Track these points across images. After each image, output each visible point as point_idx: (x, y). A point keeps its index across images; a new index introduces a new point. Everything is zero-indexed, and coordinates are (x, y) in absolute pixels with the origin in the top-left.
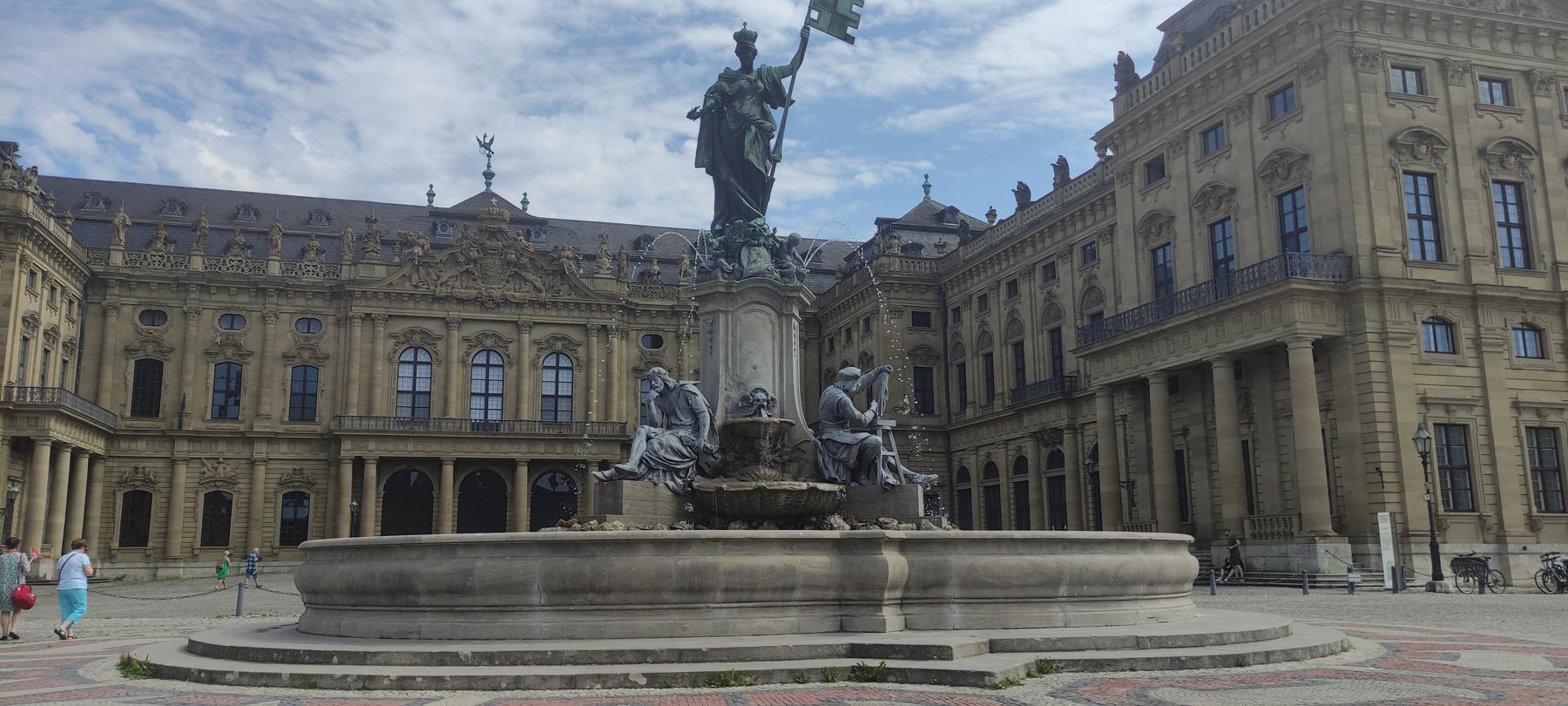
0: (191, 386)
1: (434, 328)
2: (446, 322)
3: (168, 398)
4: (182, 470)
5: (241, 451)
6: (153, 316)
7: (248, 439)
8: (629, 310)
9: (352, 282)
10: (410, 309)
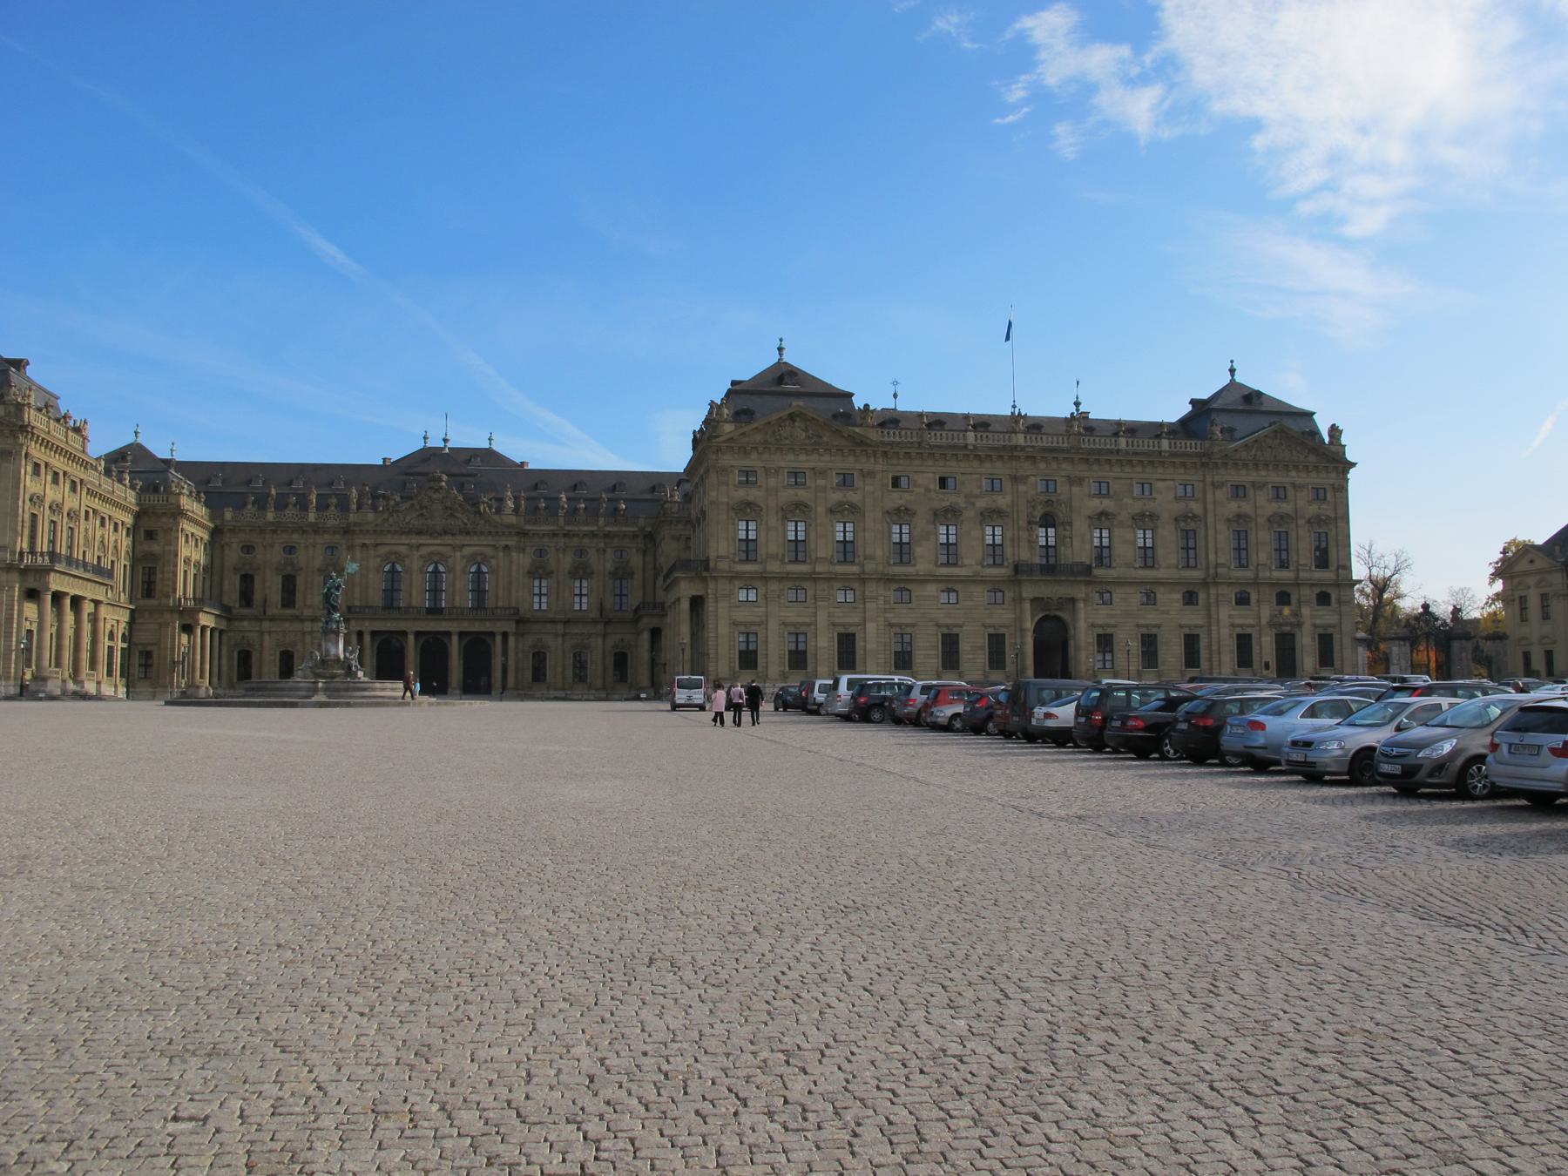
0: (269, 587)
1: (404, 550)
2: (410, 546)
3: (258, 597)
4: (266, 637)
5: (297, 626)
6: (248, 548)
7: (299, 619)
8: (522, 534)
9: (355, 524)
10: (389, 539)
